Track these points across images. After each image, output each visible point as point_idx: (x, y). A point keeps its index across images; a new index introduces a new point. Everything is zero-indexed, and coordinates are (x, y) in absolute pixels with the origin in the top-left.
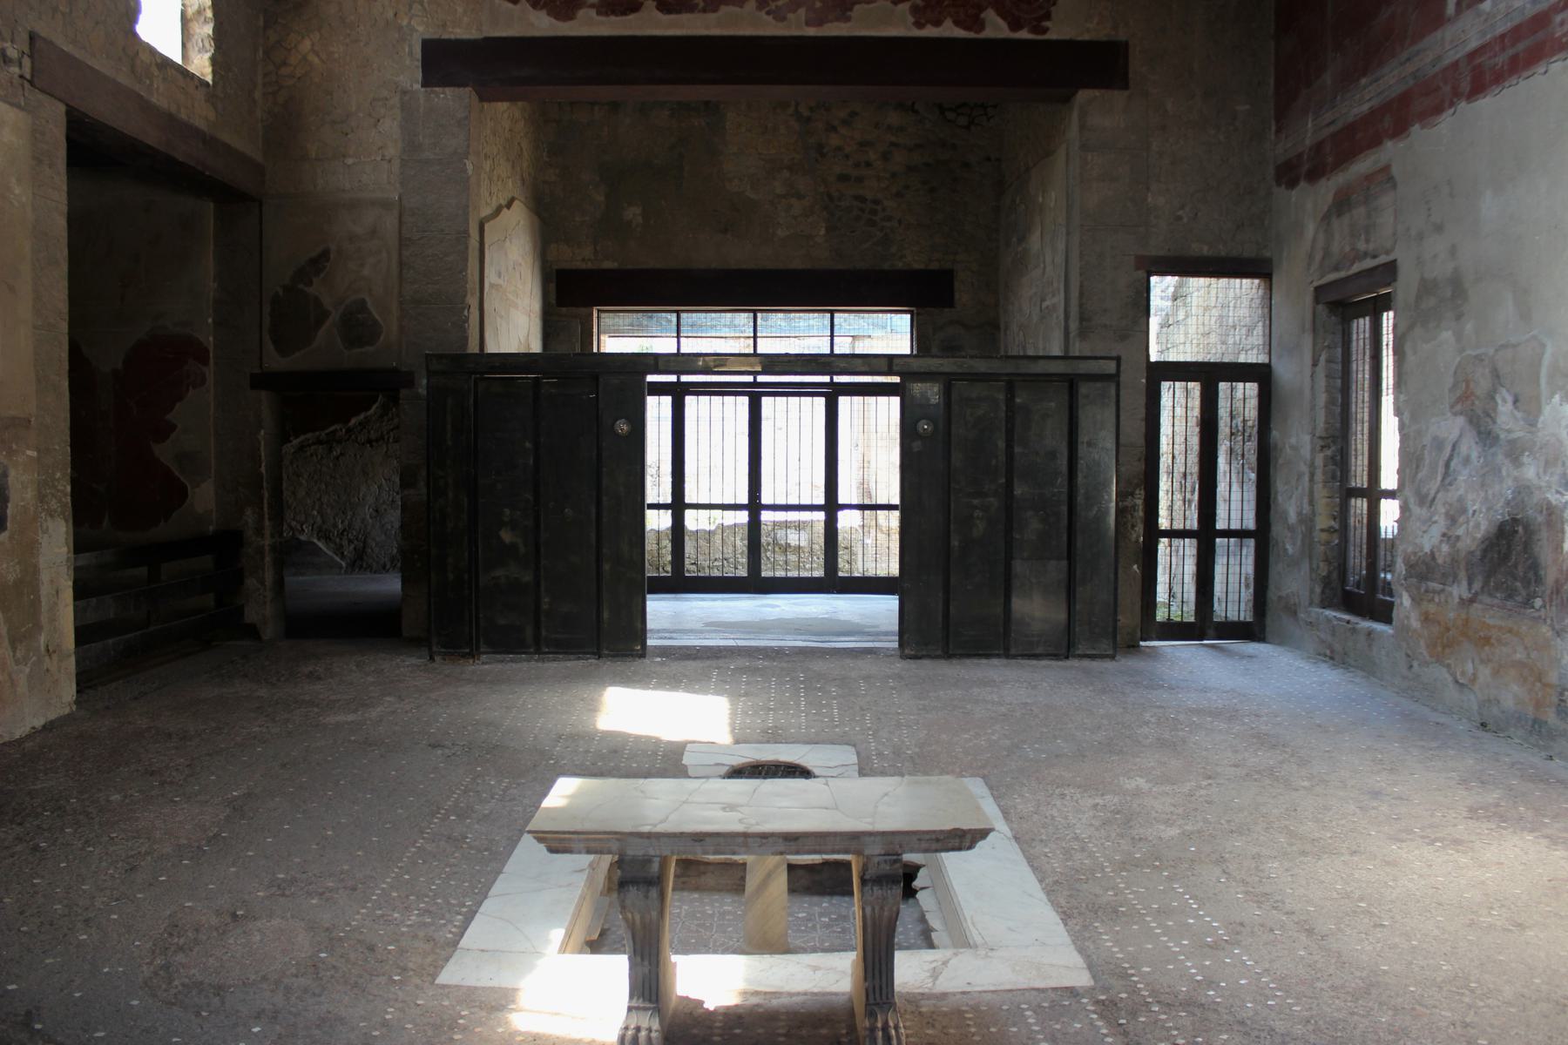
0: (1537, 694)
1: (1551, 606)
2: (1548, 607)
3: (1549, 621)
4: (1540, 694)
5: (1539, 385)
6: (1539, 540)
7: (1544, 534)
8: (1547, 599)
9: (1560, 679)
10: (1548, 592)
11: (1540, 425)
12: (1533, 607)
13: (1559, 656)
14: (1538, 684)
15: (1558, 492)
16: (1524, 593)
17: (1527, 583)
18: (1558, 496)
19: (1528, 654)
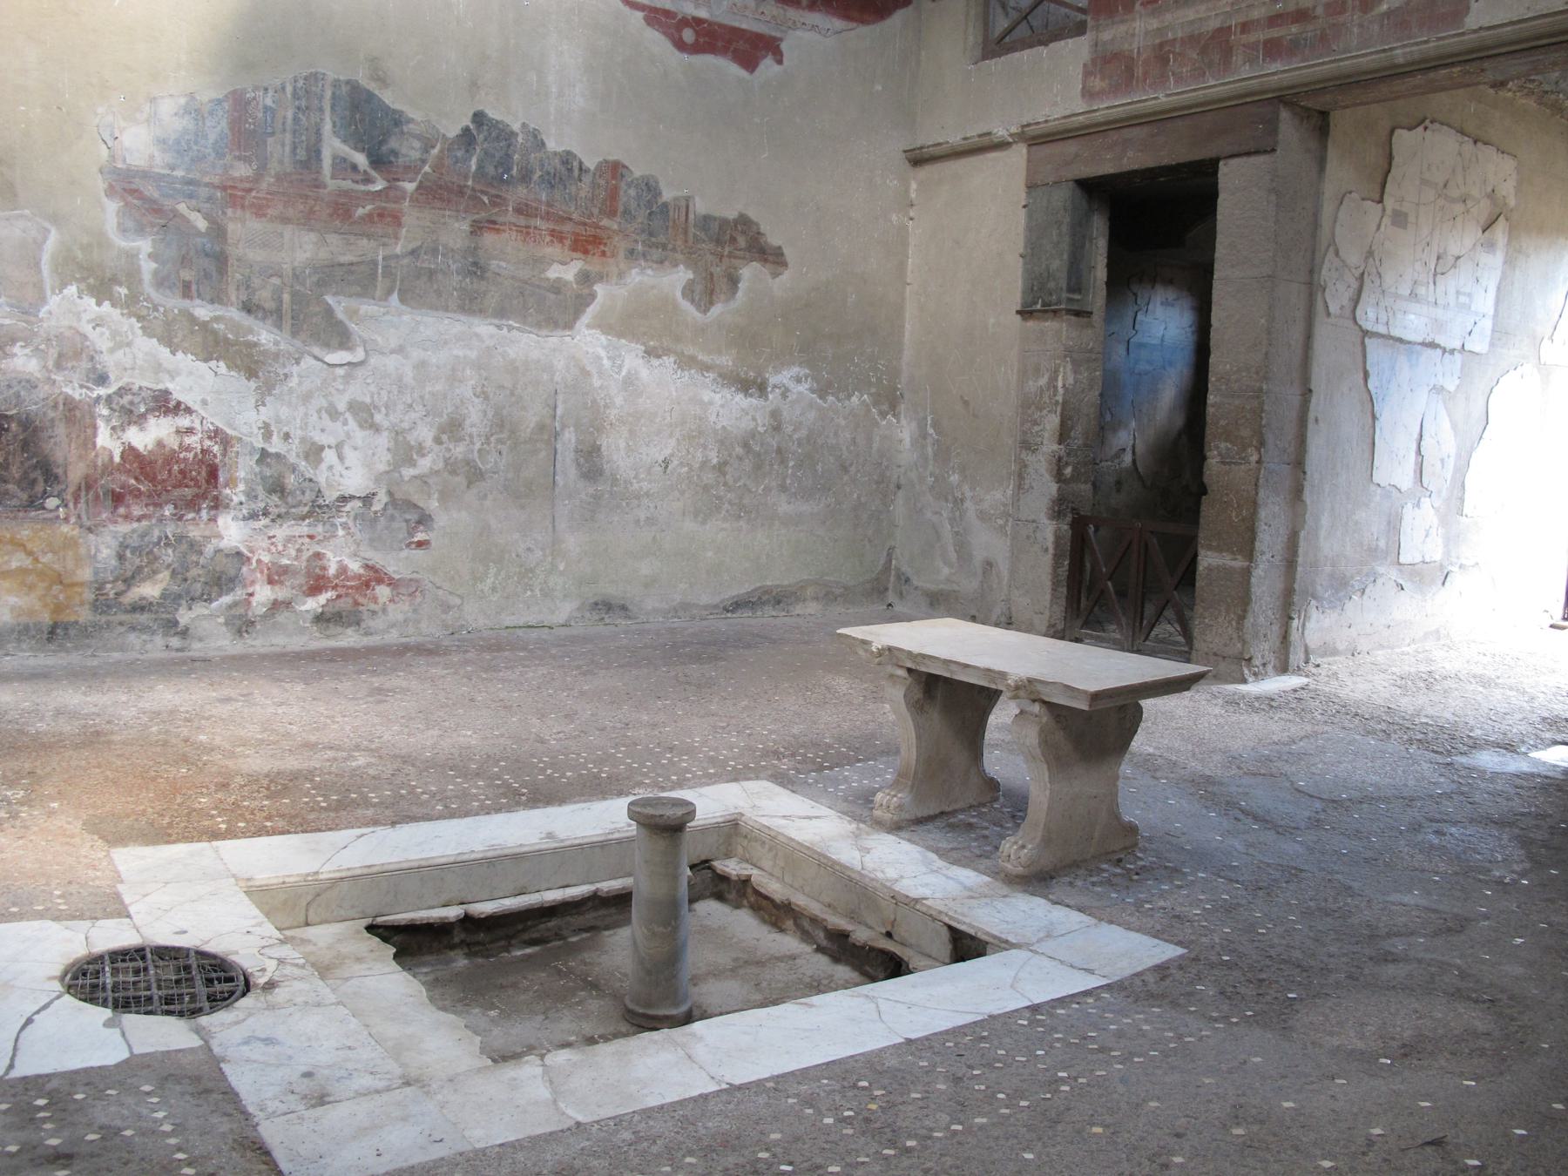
0: (56, 597)
1: (76, 503)
2: (71, 505)
3: (73, 520)
4: (61, 597)
5: (40, 272)
6: (50, 437)
7: (61, 430)
8: (69, 497)
9: (96, 573)
10: (71, 490)
11: (41, 315)
12: (44, 508)
13: (93, 552)
14: (56, 588)
15: (82, 386)
16: (25, 496)
17: (27, 483)
18: (84, 390)
19: (36, 560)
